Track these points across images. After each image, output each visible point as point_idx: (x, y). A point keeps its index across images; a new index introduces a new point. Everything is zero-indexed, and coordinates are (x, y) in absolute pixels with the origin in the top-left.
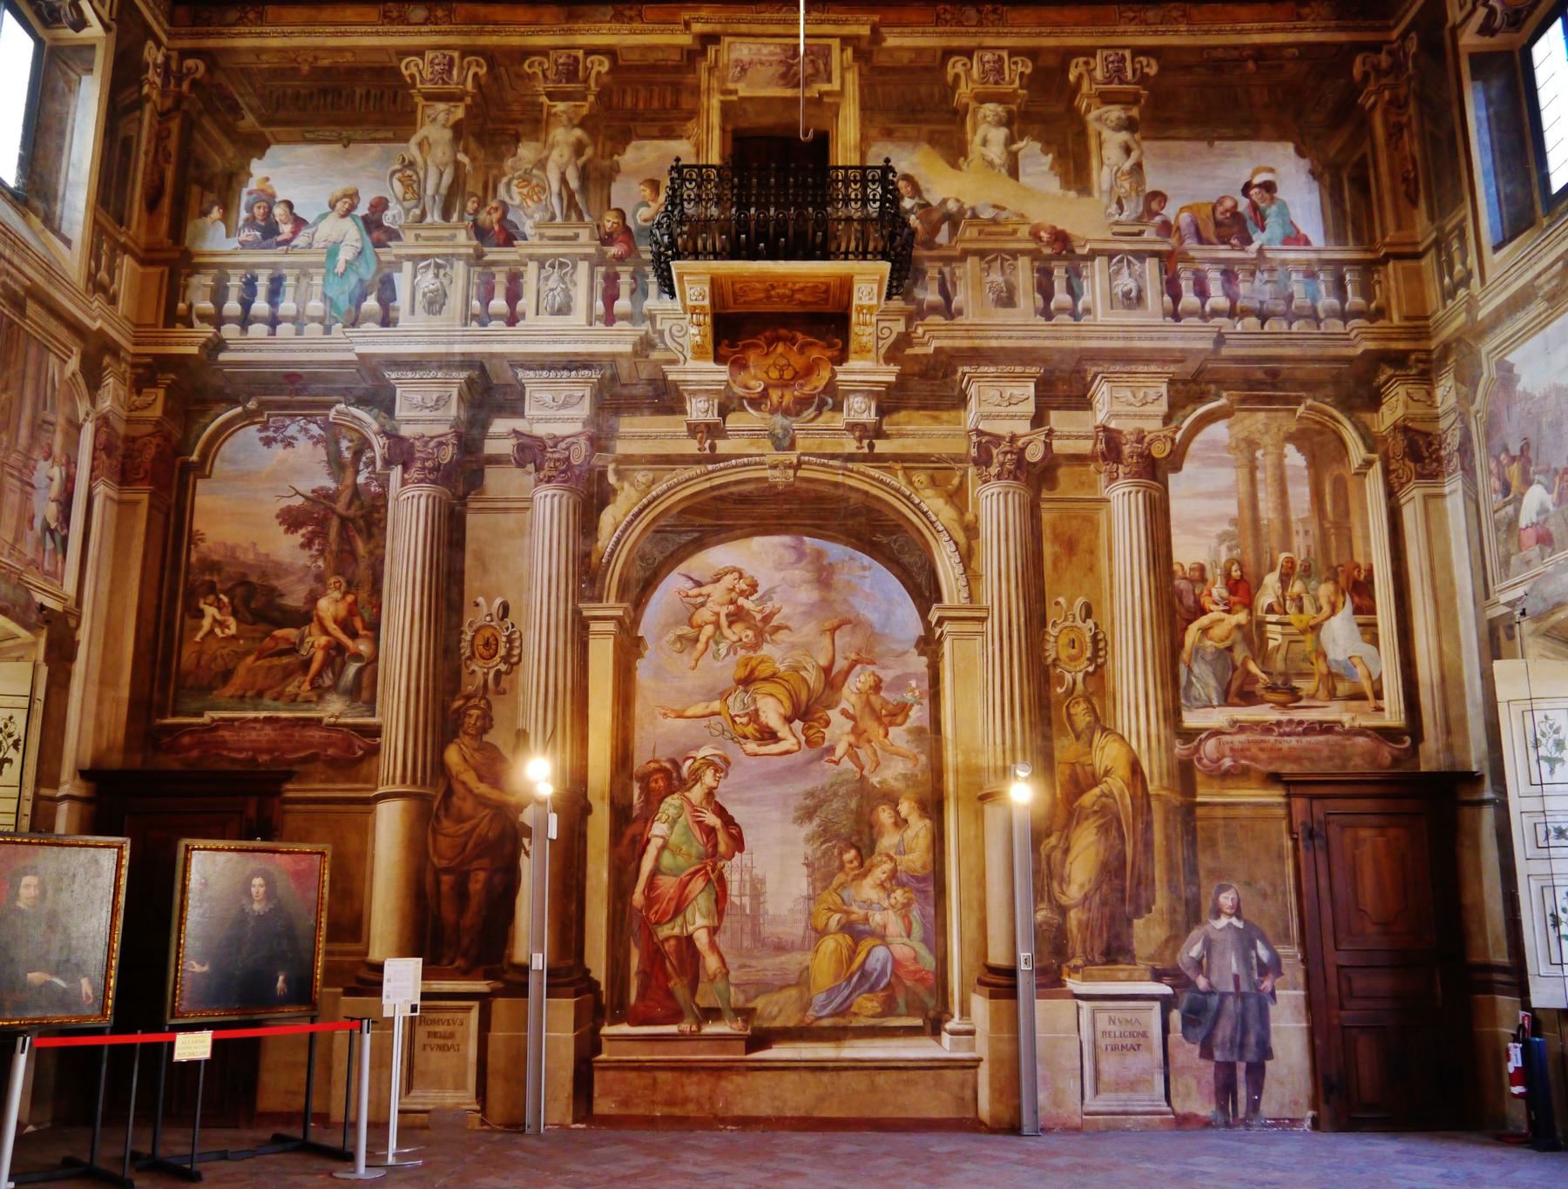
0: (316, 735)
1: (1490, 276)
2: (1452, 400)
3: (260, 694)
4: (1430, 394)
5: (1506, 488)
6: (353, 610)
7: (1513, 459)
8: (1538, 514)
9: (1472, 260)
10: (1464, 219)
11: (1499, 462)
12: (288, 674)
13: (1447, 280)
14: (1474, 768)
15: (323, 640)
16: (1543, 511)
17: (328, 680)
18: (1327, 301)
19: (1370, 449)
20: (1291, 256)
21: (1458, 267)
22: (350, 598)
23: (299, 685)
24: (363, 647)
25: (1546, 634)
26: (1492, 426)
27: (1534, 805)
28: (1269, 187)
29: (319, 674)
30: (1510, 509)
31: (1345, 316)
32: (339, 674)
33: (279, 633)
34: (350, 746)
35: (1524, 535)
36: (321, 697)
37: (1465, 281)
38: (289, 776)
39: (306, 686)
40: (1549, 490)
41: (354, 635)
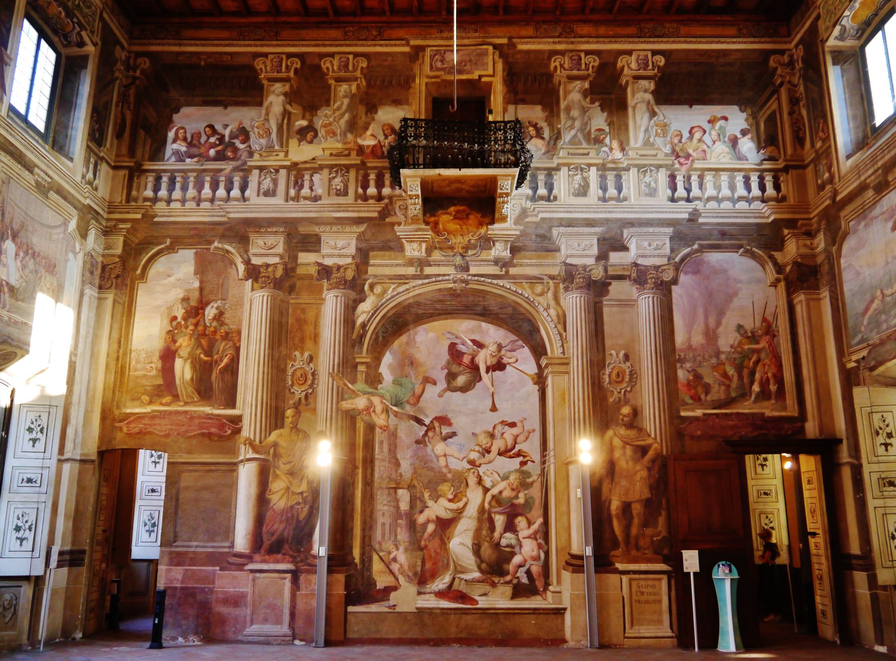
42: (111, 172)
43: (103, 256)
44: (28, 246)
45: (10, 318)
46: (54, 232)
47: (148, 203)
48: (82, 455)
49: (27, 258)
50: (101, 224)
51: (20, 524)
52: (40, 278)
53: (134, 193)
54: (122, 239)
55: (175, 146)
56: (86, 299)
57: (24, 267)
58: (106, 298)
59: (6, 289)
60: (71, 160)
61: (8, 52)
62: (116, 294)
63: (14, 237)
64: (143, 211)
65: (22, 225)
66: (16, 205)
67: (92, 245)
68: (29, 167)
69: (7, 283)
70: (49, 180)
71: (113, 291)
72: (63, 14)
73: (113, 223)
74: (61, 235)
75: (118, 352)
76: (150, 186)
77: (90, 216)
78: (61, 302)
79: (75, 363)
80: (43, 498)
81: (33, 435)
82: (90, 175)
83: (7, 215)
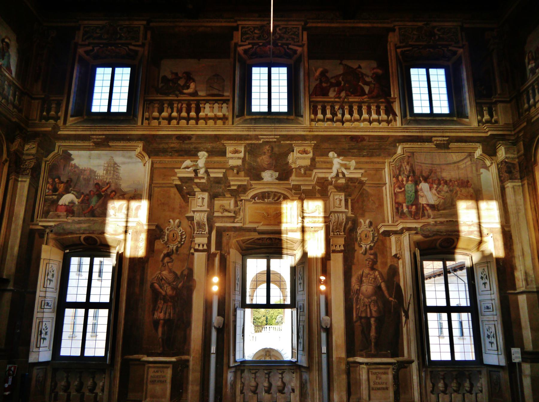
1: (68, 124)
2: (34, 151)
4: (24, 146)
5: (55, 190)
7: (62, 182)
8: (69, 203)
9: (61, 114)
10: (62, 100)
11: (54, 180)
13: (45, 113)
14: (5, 277)
16: (72, 202)
18: (11, 97)
19: (8, 156)
20: (7, 74)
21: (53, 113)
25: (56, 240)
26: (53, 169)
27: (42, 294)
28: (8, 45)
30: (55, 197)
31: (14, 106)
35: (59, 208)
37: (57, 118)
40: (77, 197)
42: (509, 105)
43: (518, 158)
44: (439, 180)
45: (436, 222)
46: (461, 163)
47: (527, 113)
48: (537, 288)
49: (441, 187)
50: (509, 140)
51: (489, 334)
52: (456, 193)
53: (521, 110)
54: (522, 143)
55: (530, 66)
56: (509, 191)
57: (439, 192)
58: (524, 184)
59: (428, 208)
60: (467, 117)
61: (392, 96)
62: (528, 180)
63: (426, 180)
64: (526, 119)
65: (431, 171)
66: (421, 163)
67: (504, 155)
68: (429, 140)
69: (428, 205)
70: (447, 138)
71: (526, 178)
72: (431, 50)
73: (516, 136)
74: (469, 163)
75: (536, 216)
76: (526, 101)
77: (494, 141)
78: (482, 199)
79: (510, 231)
80: (495, 318)
81: (484, 281)
82: (486, 117)
83: (416, 171)
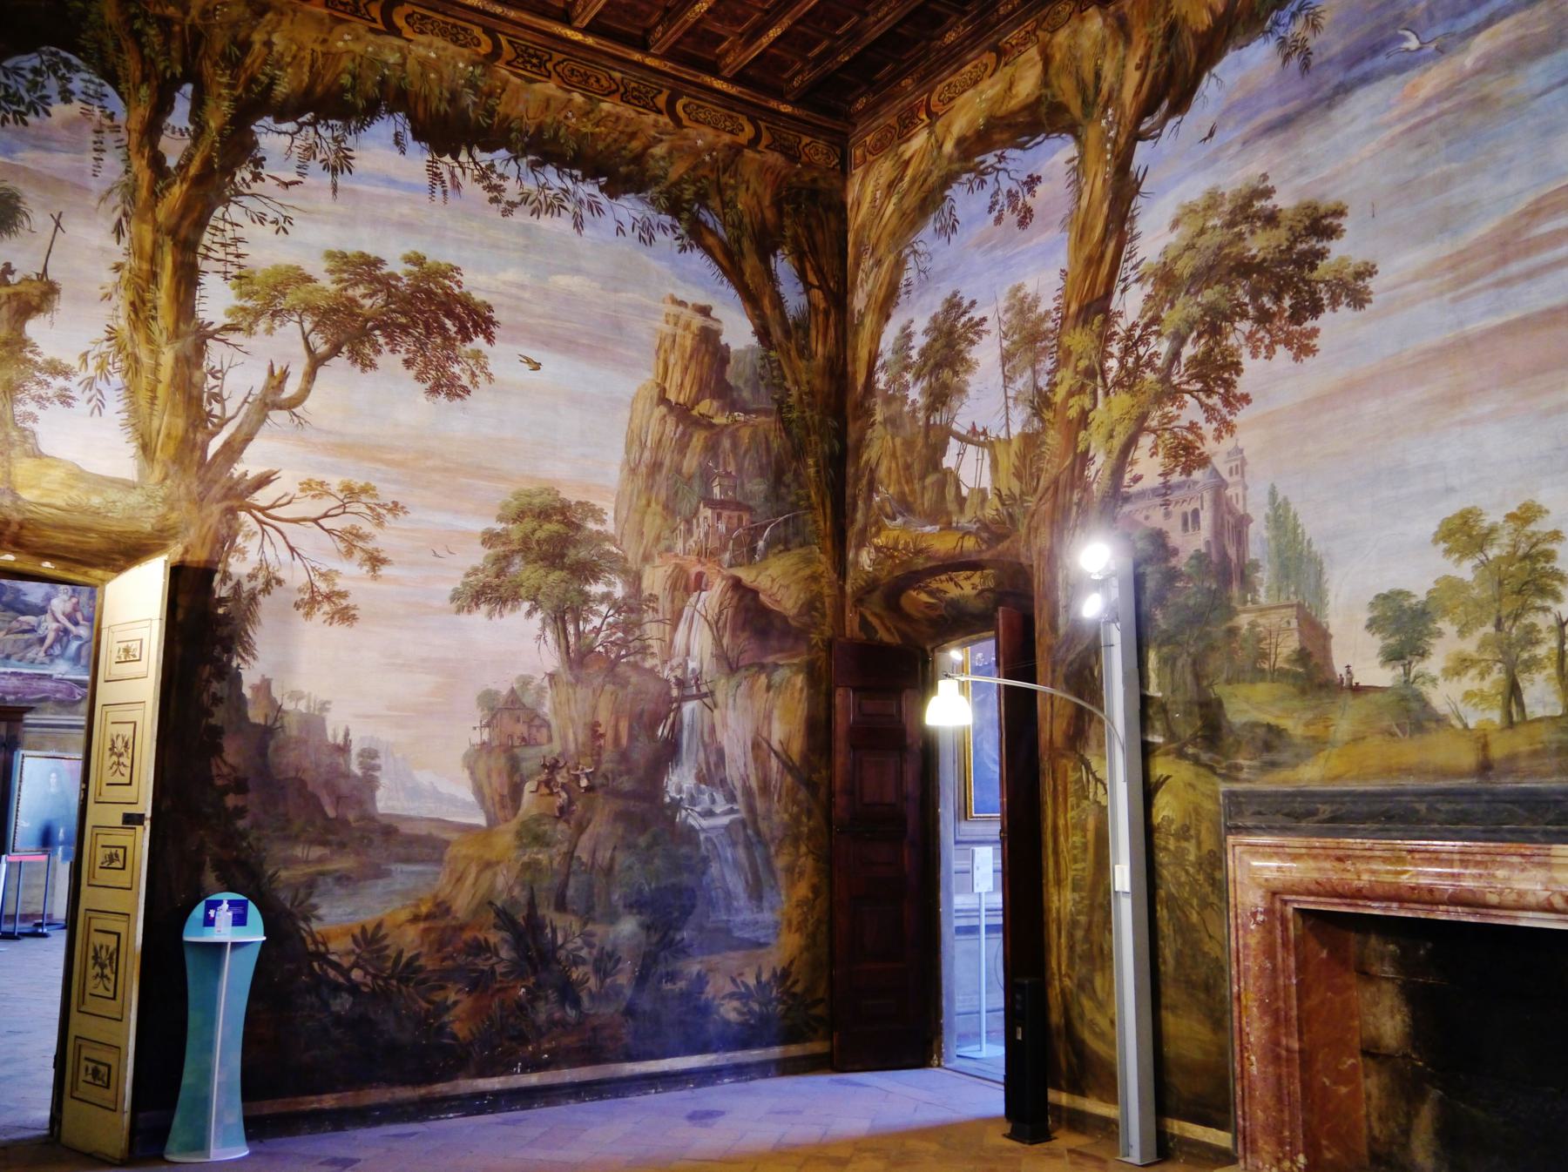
0: (48, 685)
3: (8, 657)
6: (75, 609)
12: (29, 645)
15: (55, 625)
17: (57, 650)
22: (74, 600)
23: (38, 653)
24: (83, 631)
29: (51, 647)
32: (65, 648)
33: (22, 618)
34: (72, 693)
36: (52, 661)
38: (29, 710)
39: (42, 654)
41: (76, 624)
